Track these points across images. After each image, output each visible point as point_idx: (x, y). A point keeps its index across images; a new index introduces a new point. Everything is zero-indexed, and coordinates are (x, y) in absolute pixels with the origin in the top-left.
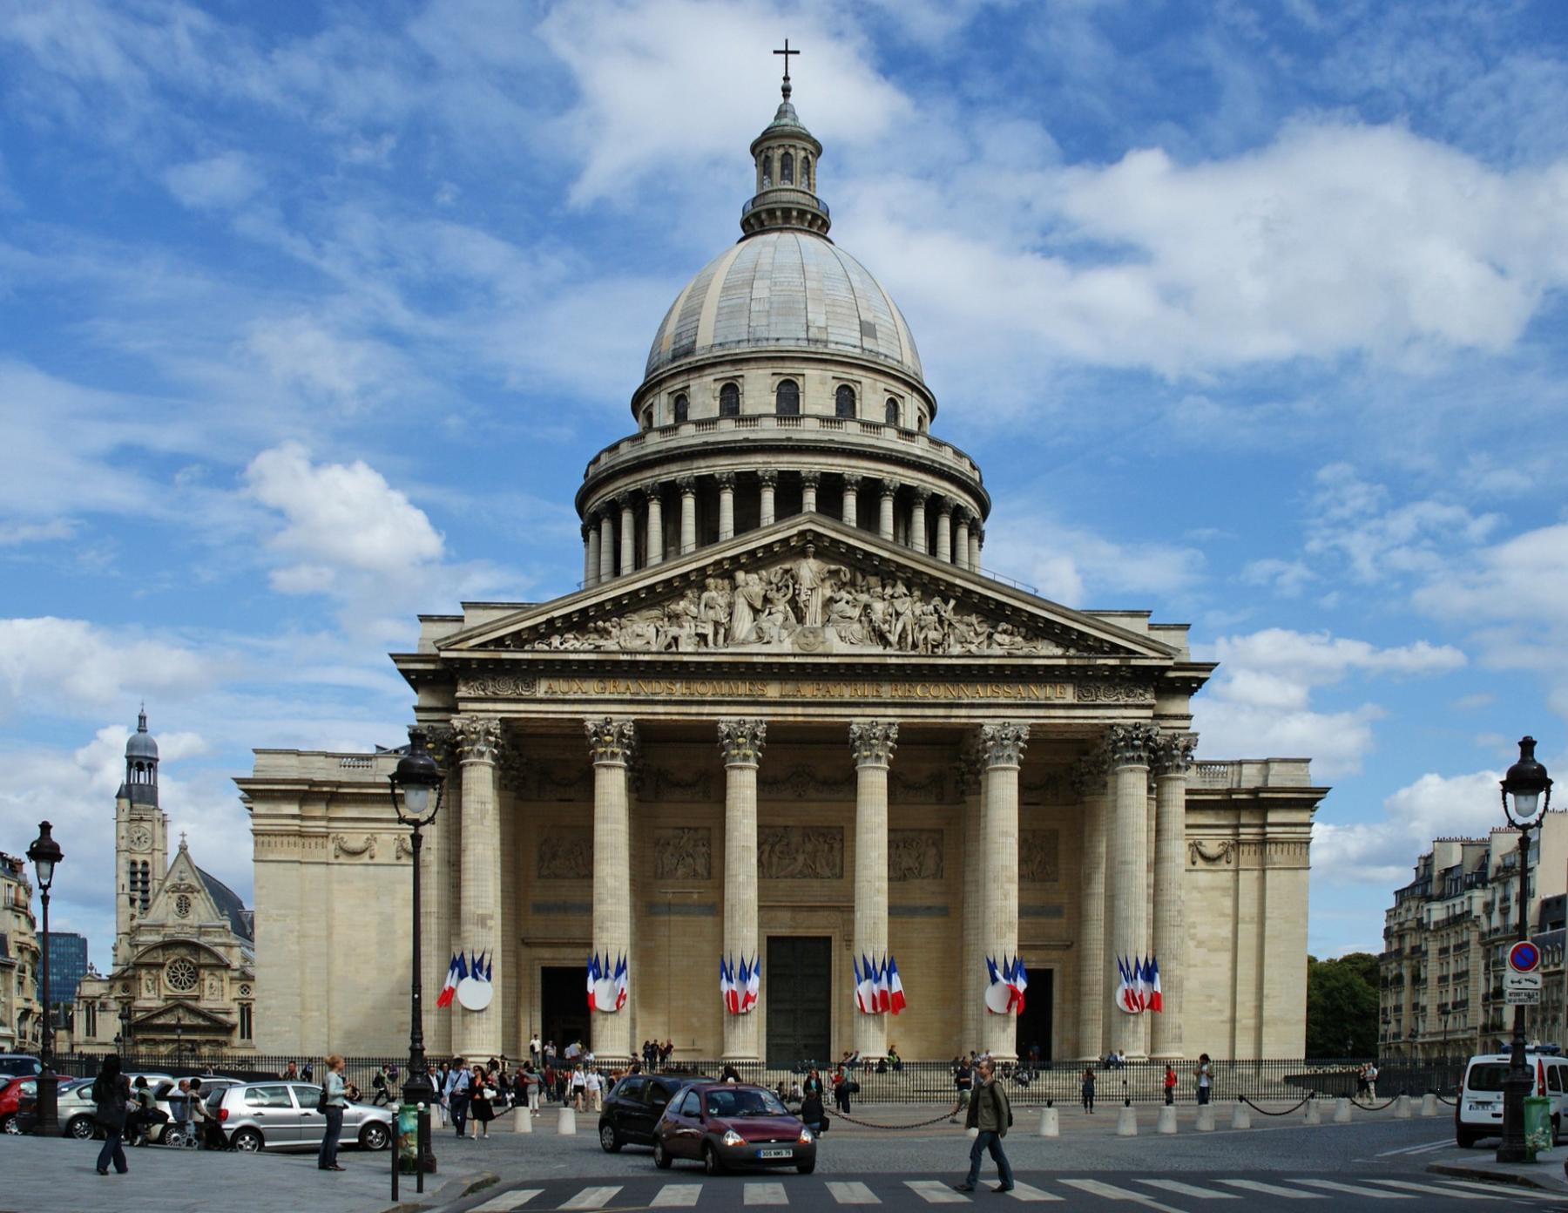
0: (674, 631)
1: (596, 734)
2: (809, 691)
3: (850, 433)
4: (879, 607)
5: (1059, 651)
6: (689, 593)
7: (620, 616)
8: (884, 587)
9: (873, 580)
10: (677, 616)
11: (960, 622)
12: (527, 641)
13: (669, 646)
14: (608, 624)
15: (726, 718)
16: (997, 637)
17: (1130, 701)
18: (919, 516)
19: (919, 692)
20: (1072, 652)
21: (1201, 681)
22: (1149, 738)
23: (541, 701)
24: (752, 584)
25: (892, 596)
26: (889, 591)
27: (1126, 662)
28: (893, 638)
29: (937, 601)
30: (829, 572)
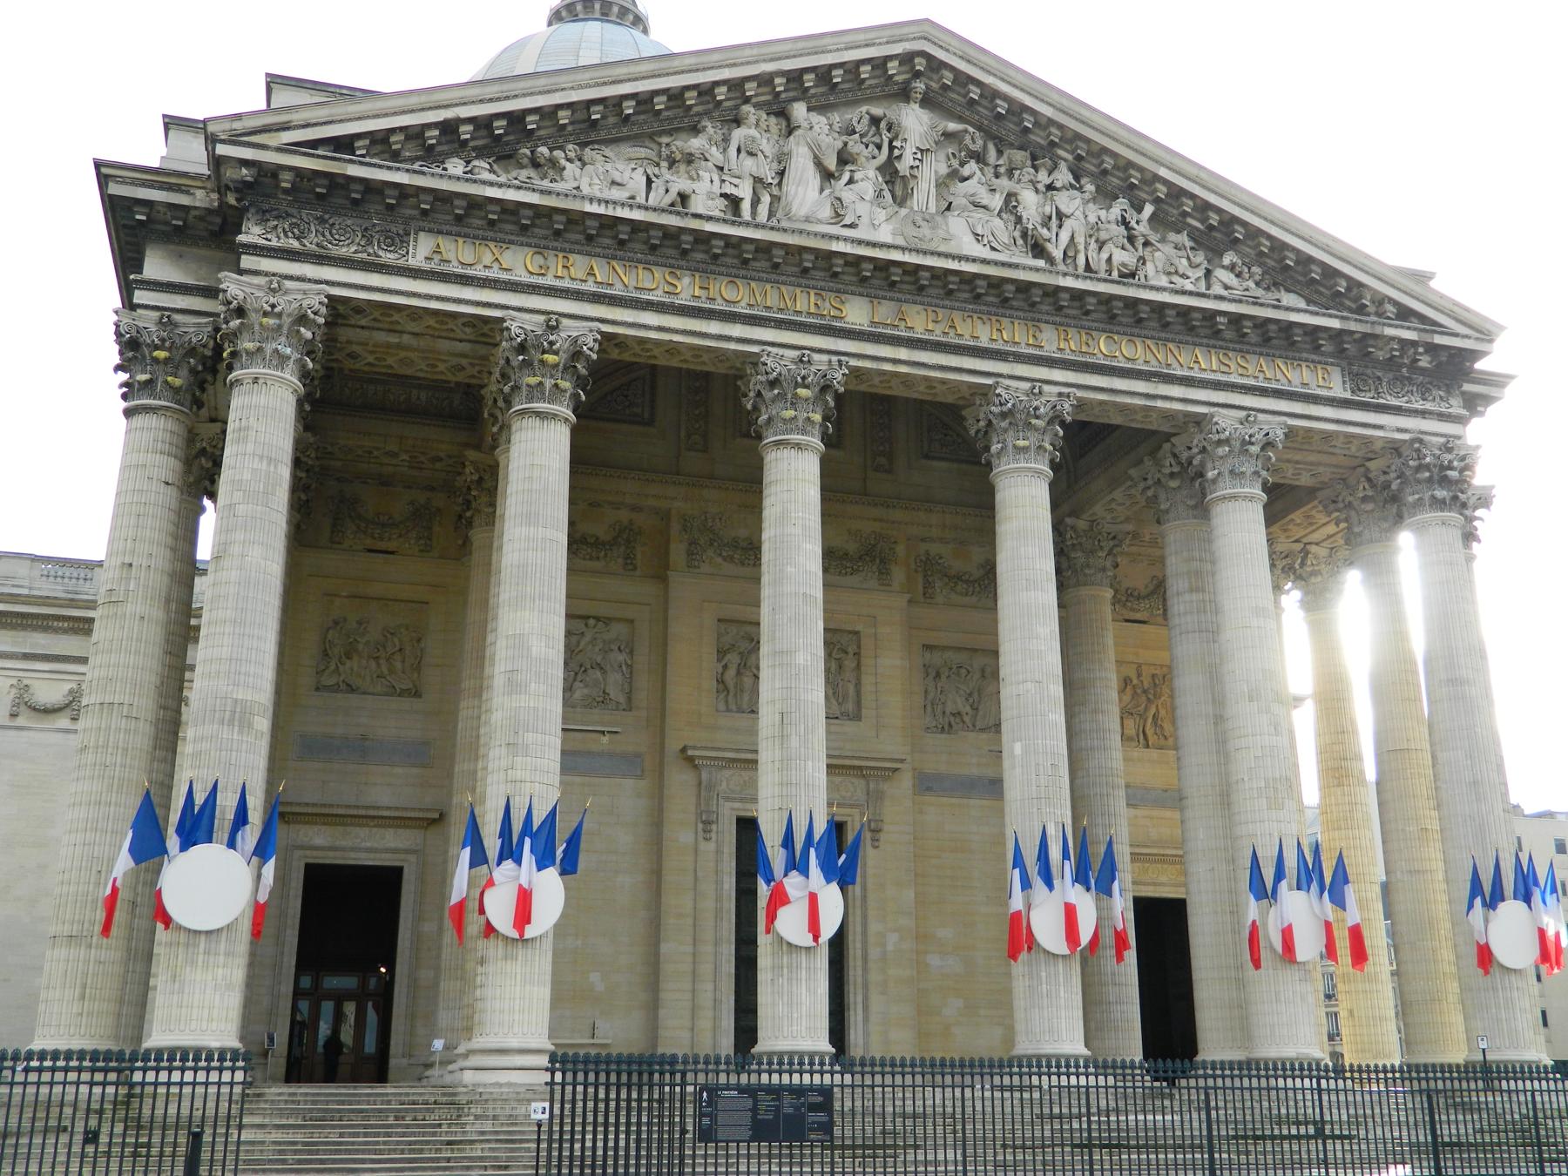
0: (680, 183)
1: (522, 348)
2: (919, 321)
4: (1030, 202)
6: (709, 124)
7: (583, 145)
9: (1020, 156)
10: (689, 159)
11: (1163, 240)
12: (395, 156)
13: (672, 205)
14: (558, 154)
15: (778, 348)
17: (1429, 406)
19: (1102, 347)
24: (818, 129)
25: (1050, 187)
26: (1043, 177)
27: (1427, 338)
28: (1057, 254)
30: (947, 135)
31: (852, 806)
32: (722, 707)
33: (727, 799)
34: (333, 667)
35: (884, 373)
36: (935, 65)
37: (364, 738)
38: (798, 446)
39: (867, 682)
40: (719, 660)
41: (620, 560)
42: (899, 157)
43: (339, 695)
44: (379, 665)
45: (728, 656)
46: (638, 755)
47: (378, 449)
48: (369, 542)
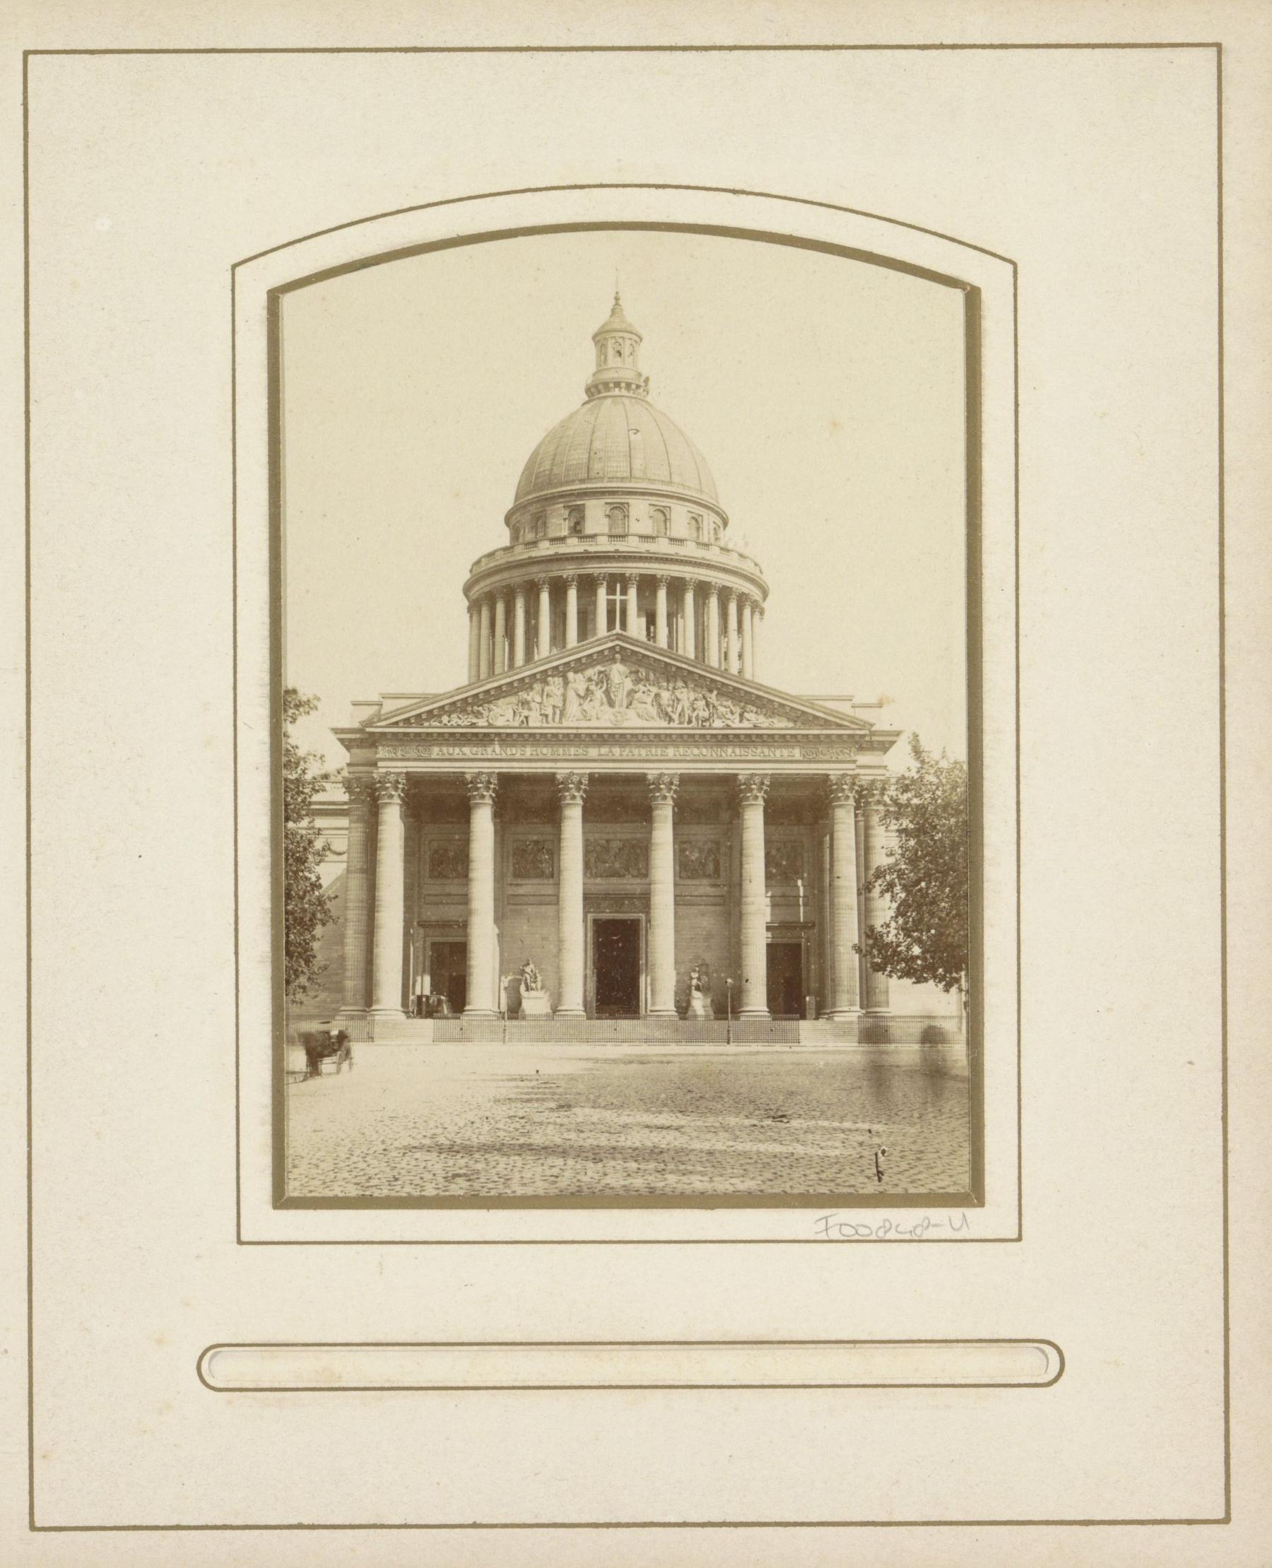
0: (526, 713)
3: (662, 547)
4: (666, 696)
5: (791, 725)
8: (668, 681)
10: (528, 703)
16: (746, 715)
18: (713, 602)
20: (799, 724)
21: (893, 743)
22: (854, 784)
23: (435, 760)
24: (578, 681)
26: (671, 685)
28: (675, 717)
29: (705, 692)
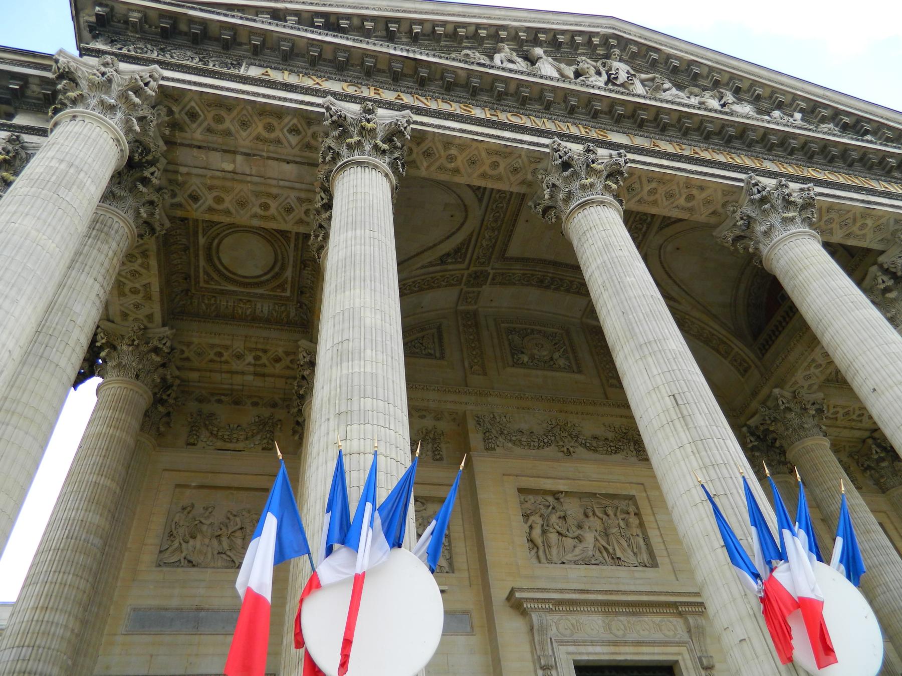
9: (696, 90)
31: (679, 644)
32: (534, 561)
33: (562, 643)
34: (176, 544)
35: (651, 177)
36: (623, 43)
37: (199, 609)
38: (602, 203)
39: (653, 534)
40: (526, 522)
41: (429, 453)
42: (616, 78)
43: (179, 570)
44: (220, 542)
45: (532, 518)
46: (466, 613)
47: (227, 348)
48: (219, 444)
